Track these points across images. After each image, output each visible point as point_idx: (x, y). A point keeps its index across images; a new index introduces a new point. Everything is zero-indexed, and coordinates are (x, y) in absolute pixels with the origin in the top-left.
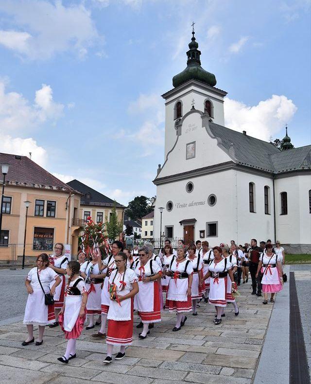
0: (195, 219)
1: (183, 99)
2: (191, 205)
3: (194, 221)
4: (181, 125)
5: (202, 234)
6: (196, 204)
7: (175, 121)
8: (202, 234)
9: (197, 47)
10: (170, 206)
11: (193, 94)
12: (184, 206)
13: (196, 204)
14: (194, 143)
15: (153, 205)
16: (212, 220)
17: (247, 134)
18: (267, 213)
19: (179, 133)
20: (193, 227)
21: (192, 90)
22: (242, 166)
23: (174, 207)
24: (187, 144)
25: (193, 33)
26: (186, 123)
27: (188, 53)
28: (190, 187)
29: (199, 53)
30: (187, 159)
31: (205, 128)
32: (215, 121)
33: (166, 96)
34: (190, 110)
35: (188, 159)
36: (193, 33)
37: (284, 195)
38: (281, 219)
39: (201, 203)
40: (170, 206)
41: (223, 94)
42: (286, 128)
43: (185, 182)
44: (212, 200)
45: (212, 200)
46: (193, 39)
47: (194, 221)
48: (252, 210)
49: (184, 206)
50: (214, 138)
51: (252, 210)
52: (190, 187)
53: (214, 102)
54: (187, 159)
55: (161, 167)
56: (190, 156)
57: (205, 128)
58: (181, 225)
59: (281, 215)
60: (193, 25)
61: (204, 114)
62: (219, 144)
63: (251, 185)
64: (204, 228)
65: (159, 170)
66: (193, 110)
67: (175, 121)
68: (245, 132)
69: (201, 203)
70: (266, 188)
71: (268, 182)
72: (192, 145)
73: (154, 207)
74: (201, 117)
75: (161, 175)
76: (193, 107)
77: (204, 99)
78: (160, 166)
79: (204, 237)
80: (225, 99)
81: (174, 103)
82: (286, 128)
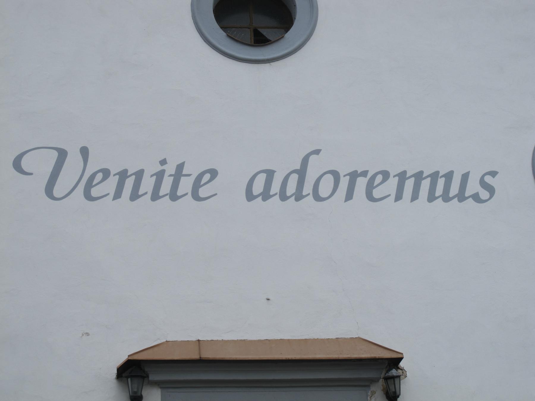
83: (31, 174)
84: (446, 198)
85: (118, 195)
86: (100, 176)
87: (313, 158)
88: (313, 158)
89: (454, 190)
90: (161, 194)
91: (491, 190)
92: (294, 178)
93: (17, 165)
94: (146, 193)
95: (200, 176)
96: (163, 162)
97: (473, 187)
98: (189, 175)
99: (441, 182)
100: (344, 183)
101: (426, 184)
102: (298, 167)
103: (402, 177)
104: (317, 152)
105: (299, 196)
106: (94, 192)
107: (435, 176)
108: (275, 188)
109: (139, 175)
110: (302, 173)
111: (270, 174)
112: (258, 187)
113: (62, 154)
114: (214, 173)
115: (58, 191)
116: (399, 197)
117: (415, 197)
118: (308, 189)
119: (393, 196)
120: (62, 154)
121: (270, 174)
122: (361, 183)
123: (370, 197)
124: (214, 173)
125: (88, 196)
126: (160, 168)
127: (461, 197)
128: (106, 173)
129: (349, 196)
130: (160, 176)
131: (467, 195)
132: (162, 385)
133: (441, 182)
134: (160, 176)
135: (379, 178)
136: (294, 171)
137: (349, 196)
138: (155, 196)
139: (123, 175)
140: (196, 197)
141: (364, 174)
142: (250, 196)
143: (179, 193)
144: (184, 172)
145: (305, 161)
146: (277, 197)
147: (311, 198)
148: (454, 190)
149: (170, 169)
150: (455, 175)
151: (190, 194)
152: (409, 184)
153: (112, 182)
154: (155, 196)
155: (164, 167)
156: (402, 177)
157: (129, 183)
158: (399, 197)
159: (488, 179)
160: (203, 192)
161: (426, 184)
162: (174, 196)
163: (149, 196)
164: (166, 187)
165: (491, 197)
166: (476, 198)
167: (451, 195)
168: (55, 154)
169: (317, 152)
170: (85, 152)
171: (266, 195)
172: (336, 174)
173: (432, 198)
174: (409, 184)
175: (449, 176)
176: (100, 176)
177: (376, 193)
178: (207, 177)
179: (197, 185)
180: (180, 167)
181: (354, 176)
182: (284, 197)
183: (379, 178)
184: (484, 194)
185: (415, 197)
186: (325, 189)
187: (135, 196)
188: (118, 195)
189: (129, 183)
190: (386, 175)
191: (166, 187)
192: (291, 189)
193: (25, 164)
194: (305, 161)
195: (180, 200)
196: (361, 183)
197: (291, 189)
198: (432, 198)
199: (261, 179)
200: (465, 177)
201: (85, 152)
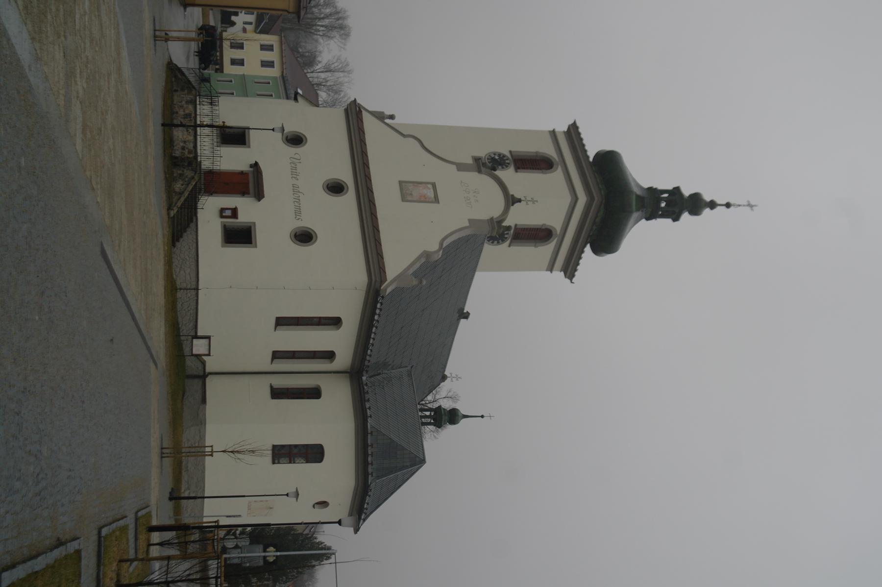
0: (263, 197)
1: (557, 175)
2: (295, 189)
3: (259, 195)
4: (480, 171)
5: (228, 213)
6: (297, 200)
7: (508, 155)
8: (228, 213)
9: (689, 213)
10: (296, 140)
11: (567, 199)
12: (294, 174)
13: (297, 200)
14: (436, 200)
15: (299, 98)
16: (260, 235)
17: (463, 321)
18: (277, 355)
19: (461, 167)
20: (243, 192)
21: (575, 199)
22: (376, 302)
23: (293, 150)
25: (728, 205)
26: (483, 182)
27: (676, 191)
28: (336, 188)
29: (676, 219)
30: (401, 183)
31: (467, 224)
32: (489, 250)
33: (573, 132)
34: (511, 193)
35: (401, 189)
36: (728, 205)
37: (314, 393)
38: (263, 386)
39: (298, 212)
40: (296, 140)
41: (570, 270)
42: (482, 417)
43: (346, 176)
44: (304, 237)
45: (304, 237)
46: (712, 205)
47: (259, 195)
48: (281, 322)
49: (294, 174)
50: (441, 244)
51: (281, 322)
52: (336, 188)
53: (547, 250)
54: (401, 183)
55: (387, 121)
56: (407, 191)
57: (467, 224)
58: (251, 166)
59: (271, 387)
60: (750, 206)
61: (500, 222)
62: (426, 255)
63: (336, 322)
64: (243, 218)
65: (380, 116)
66: (511, 200)
67: (508, 155)
68: (466, 316)
69: (298, 212)
70: (330, 355)
71: (344, 358)
72: (431, 194)
73: (296, 99)
74: (492, 219)
75: (369, 123)
76: (520, 201)
77: (557, 225)
78: (392, 117)
79: (222, 217)
80: (559, 275)
82: (482, 417)
91: (299, 219)
93: (296, 154)
97: (298, 217)
106: (292, 164)
109: (296, 170)
110: (299, 192)
111: (298, 188)
120: (300, 160)
121: (298, 188)
122: (298, 201)
123: (294, 202)
130: (296, 172)
132: (254, 171)
134: (296, 172)
145: (301, 193)
149: (298, 174)
166: (296, 217)
168: (299, 158)
170: (300, 163)
171: (293, 187)
172: (299, 197)
173: (295, 210)
175: (300, 214)
180: (298, 175)
181: (299, 200)
190: (300, 204)
194: (301, 193)
196: (298, 201)
201: (300, 163)
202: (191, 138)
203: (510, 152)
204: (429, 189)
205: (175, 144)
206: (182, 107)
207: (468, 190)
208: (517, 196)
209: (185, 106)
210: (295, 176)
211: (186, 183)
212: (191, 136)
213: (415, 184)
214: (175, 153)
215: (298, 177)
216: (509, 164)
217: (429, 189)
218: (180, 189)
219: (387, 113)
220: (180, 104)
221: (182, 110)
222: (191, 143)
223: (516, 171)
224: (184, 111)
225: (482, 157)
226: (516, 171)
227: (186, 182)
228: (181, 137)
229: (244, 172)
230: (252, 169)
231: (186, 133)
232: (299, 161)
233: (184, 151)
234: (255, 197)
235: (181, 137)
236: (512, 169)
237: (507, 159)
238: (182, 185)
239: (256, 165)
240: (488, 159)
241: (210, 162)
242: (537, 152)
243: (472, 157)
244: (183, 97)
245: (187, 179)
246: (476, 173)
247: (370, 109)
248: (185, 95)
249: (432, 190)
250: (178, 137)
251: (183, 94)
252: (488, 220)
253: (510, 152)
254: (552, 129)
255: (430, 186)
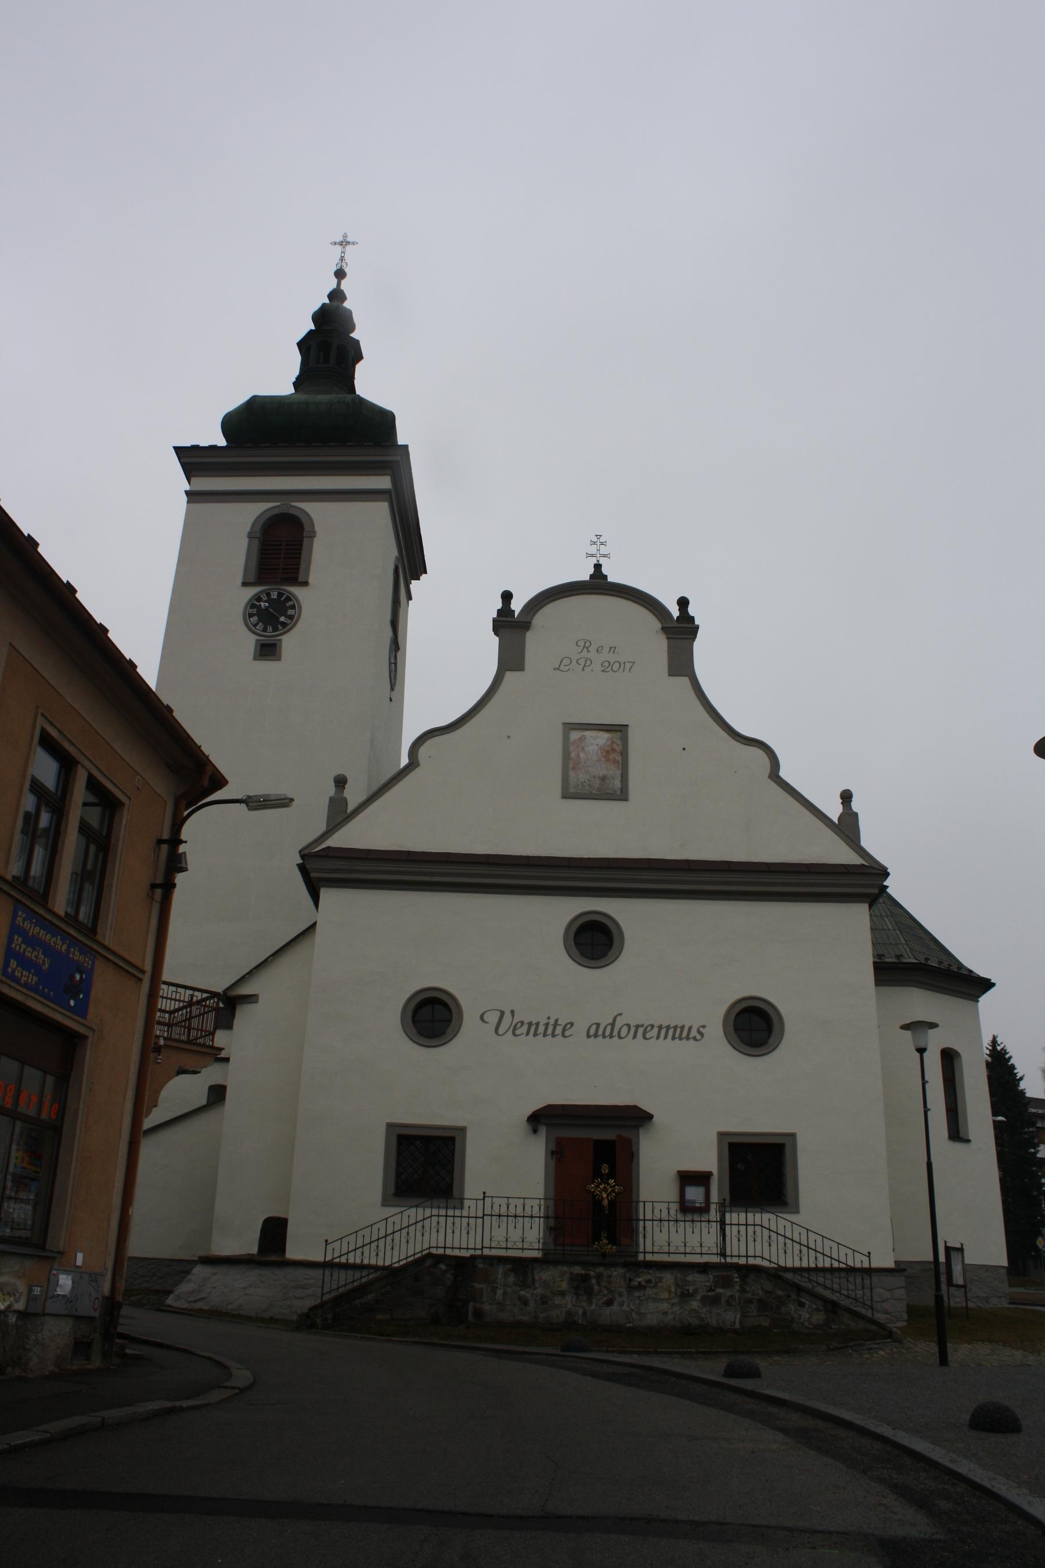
0: (635, 1108)
2: (595, 1032)
6: (641, 1031)
7: (253, 591)
8: (694, 1194)
13: (641, 1031)
24: (570, 727)
25: (340, 274)
34: (588, 578)
36: (340, 274)
39: (679, 1033)
46: (337, 295)
67: (253, 591)
69: (679, 1033)
72: (603, 738)
78: (341, 782)
81: (252, 512)
83: (488, 1023)
84: (680, 1038)
85: (528, 1034)
86: (520, 1024)
87: (619, 1018)
88: (619, 1018)
89: (684, 1035)
90: (548, 1034)
91: (702, 1034)
92: (609, 1028)
93: (482, 1018)
94: (540, 1033)
95: (566, 1025)
96: (549, 1018)
97: (694, 1033)
98: (560, 1025)
99: (679, 1030)
100: (633, 1030)
101: (671, 1031)
102: (611, 1021)
103: (660, 1027)
104: (620, 1014)
105: (611, 1036)
106: (518, 1032)
107: (675, 1027)
108: (600, 1032)
109: (538, 1024)
110: (613, 1024)
111: (598, 1025)
112: (592, 1032)
113: (502, 1013)
114: (572, 1024)
115: (501, 1031)
116: (658, 1037)
117: (666, 1037)
118: (615, 1033)
119: (655, 1037)
120: (502, 1013)
121: (598, 1025)
122: (641, 1030)
124: (572, 1024)
125: (514, 1034)
126: (547, 1021)
127: (688, 1038)
128: (522, 1023)
129: (635, 1037)
130: (547, 1025)
131: (691, 1036)
133: (679, 1030)
134: (547, 1025)
135: (649, 1028)
136: (610, 1024)
137: (635, 1037)
138: (545, 1035)
139: (530, 1024)
140: (564, 1036)
141: (642, 1026)
142: (588, 1036)
143: (556, 1034)
144: (559, 1023)
145: (615, 1019)
146: (601, 1036)
147: (617, 1037)
148: (684, 1035)
149: (552, 1022)
150: (685, 1027)
151: (561, 1035)
152: (663, 1032)
153: (525, 1027)
154: (545, 1035)
155: (549, 1021)
156: (660, 1027)
157: (533, 1028)
158: (658, 1037)
159: (701, 1029)
160: (567, 1033)
161: (671, 1031)
162: (553, 1035)
163: (542, 1034)
164: (550, 1031)
165: (701, 1039)
166: (695, 1039)
167: (683, 1037)
168: (499, 1013)
169: (620, 1014)
170: (512, 1012)
171: (596, 1035)
172: (629, 1026)
174: (663, 1032)
175: (682, 1028)
176: (520, 1024)
177: (648, 1036)
178: (569, 1026)
179: (564, 1030)
180: (557, 1021)
181: (637, 1027)
182: (604, 1037)
183: (649, 1028)
184: (699, 1037)
185: (666, 1037)
186: (624, 1033)
187: (535, 1034)
188: (528, 1034)
189: (533, 1028)
190: (652, 1026)
191: (550, 1031)
192: (608, 1032)
193: (485, 1017)
194: (615, 1019)
195: (557, 1037)
196: (641, 1030)
197: (608, 1032)
198: (673, 1038)
199: (594, 1028)
200: (690, 1028)
201: (512, 1012)
202: (668, 1278)
203: (245, 584)
204: (582, 739)
205: (695, 1322)
206: (544, 1301)
207: (582, 662)
208: (592, 571)
209: (539, 1291)
210: (559, 1030)
211: (794, 1296)
212: (660, 1279)
213: (571, 765)
214: (734, 1323)
215: (562, 1022)
216: (280, 595)
217: (582, 739)
218: (817, 1310)
219: (331, 790)
220: (532, 1305)
221: (557, 1300)
222: (690, 1278)
223: (305, 584)
224: (563, 1294)
225: (257, 641)
226: (305, 584)
227: (789, 1296)
228: (665, 1306)
229: (553, 1147)
230: (543, 1130)
231: (649, 1292)
232: (508, 1015)
233: (723, 1300)
234: (637, 1127)
235: (665, 1306)
236: (296, 591)
237: (268, 595)
238: (801, 1305)
239: (537, 1119)
240: (265, 630)
241: (657, 1230)
242: (250, 536)
243: (255, 659)
244: (504, 1293)
245: (780, 1293)
246: (529, 635)
247: (323, 828)
248: (494, 1290)
249: (587, 733)
250: (665, 1313)
251: (495, 1293)
252: (667, 638)
253: (245, 584)
254: (185, 498)
255: (574, 735)
